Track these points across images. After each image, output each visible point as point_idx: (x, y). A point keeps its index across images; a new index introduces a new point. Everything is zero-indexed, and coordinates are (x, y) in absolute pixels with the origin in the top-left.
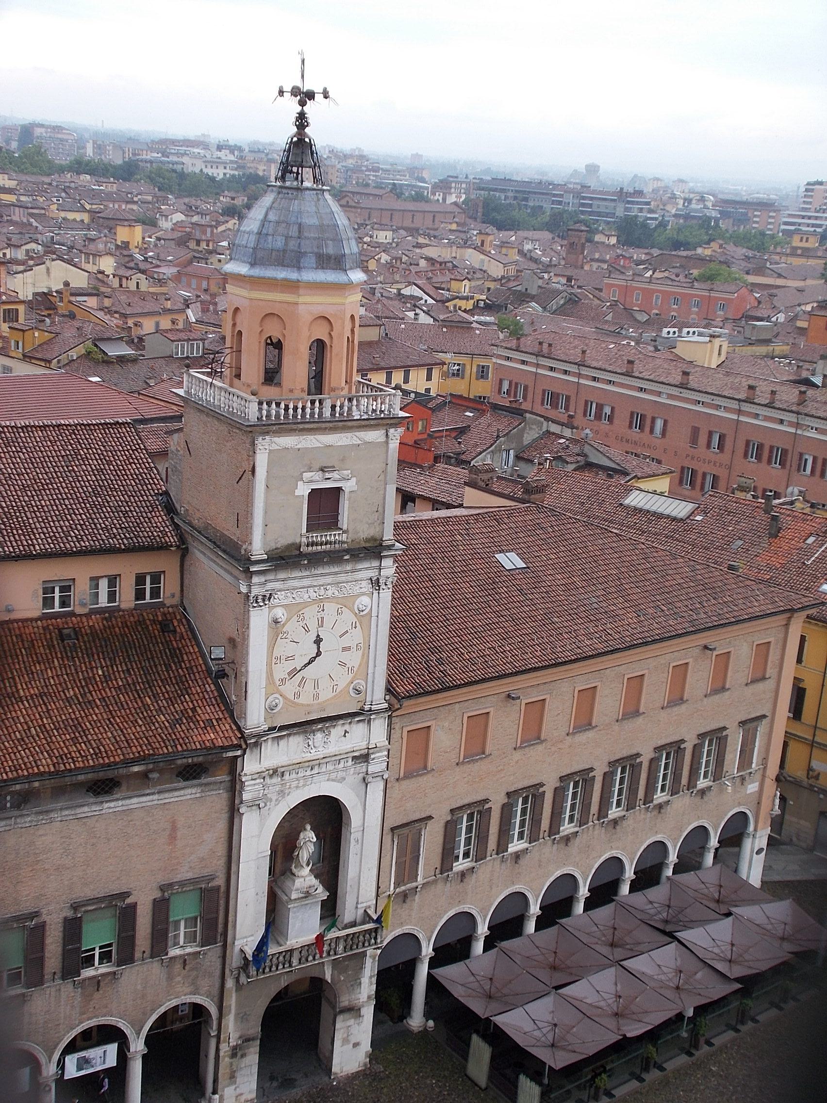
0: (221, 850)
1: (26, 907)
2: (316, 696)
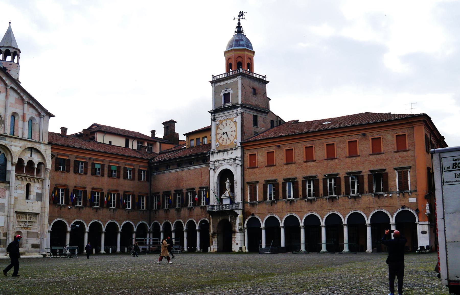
1: (181, 188)
2: (226, 143)
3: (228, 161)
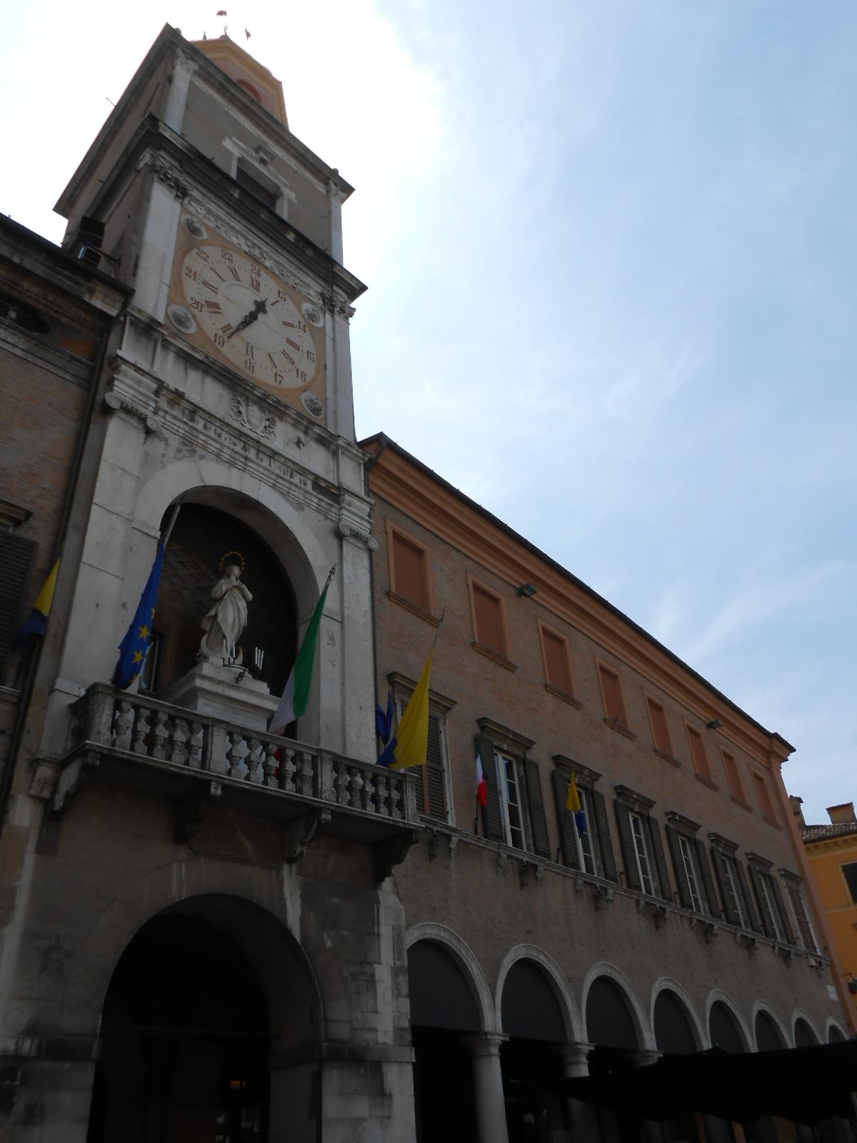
0: (51, 479)
3: (276, 467)
